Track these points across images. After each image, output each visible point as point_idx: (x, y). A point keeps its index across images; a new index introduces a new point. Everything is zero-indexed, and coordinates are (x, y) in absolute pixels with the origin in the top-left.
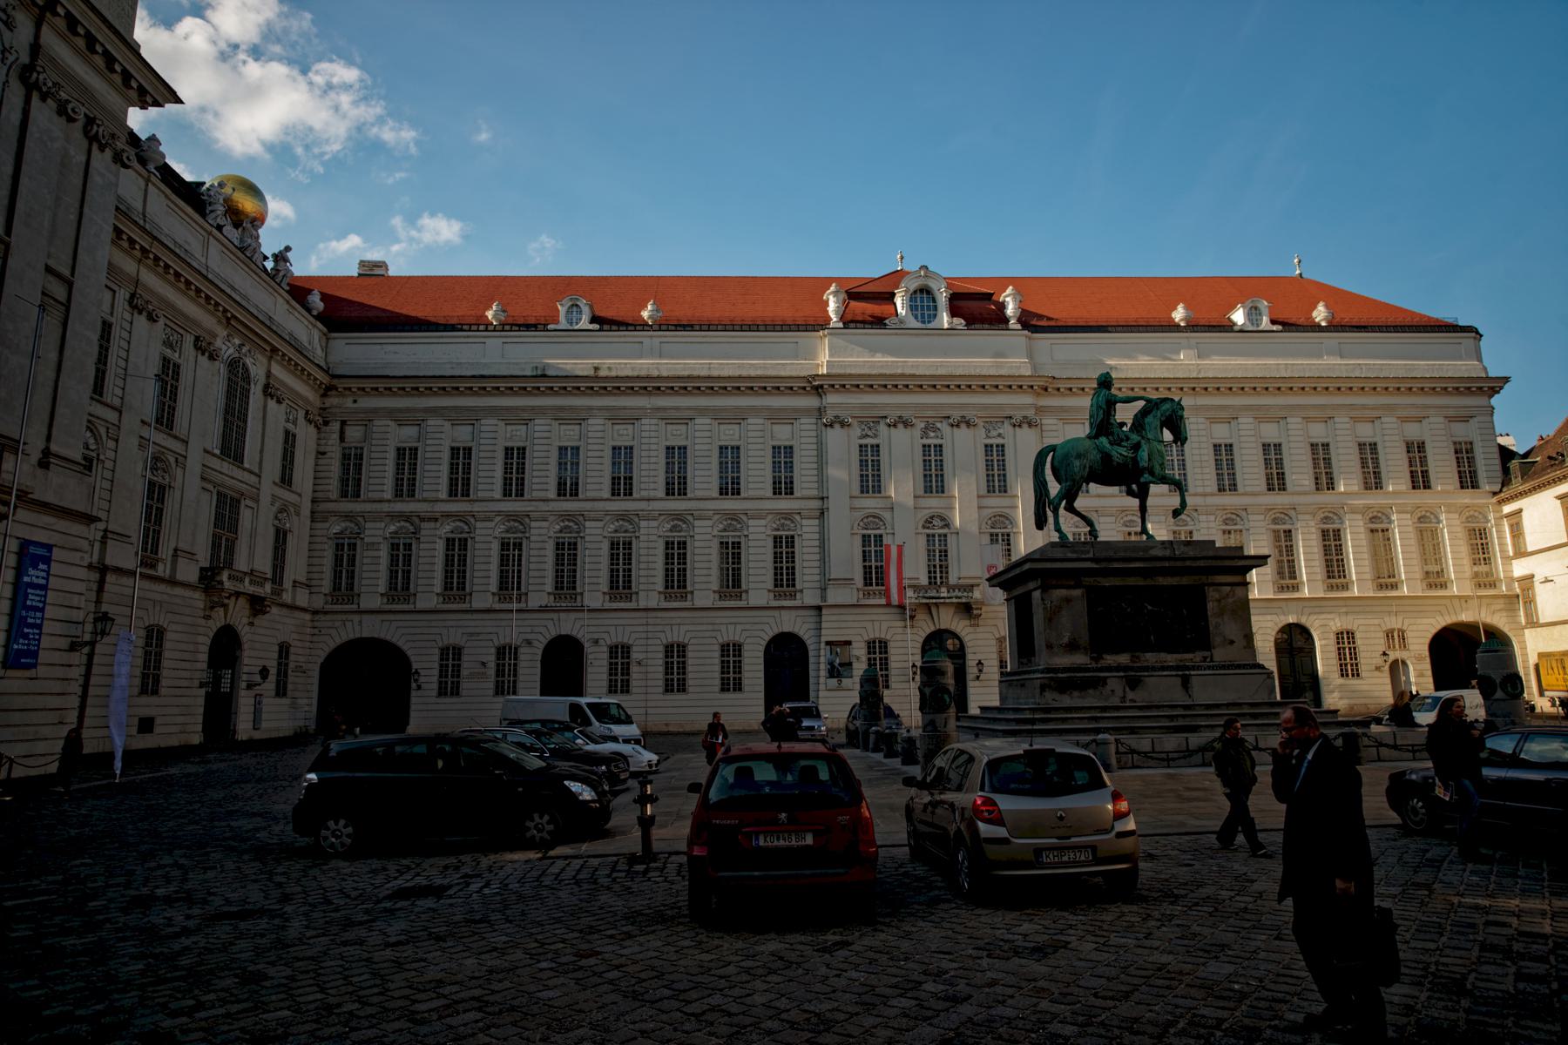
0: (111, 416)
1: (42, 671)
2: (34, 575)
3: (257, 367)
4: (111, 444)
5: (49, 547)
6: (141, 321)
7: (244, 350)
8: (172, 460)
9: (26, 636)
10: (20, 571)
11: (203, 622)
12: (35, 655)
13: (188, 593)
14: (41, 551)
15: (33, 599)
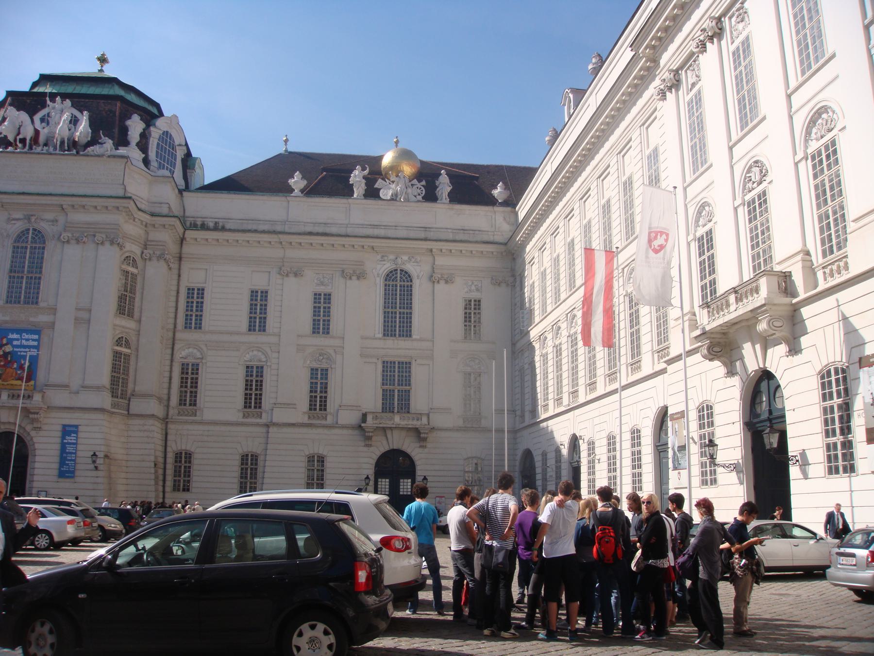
0: (273, 339)
1: (77, 479)
2: (70, 439)
3: (418, 270)
4: (275, 355)
5: (77, 426)
6: (292, 281)
7: (399, 260)
8: (331, 352)
9: (68, 465)
10: (63, 438)
11: (366, 449)
12: (73, 472)
13: (345, 432)
14: (74, 429)
15: (69, 449)
